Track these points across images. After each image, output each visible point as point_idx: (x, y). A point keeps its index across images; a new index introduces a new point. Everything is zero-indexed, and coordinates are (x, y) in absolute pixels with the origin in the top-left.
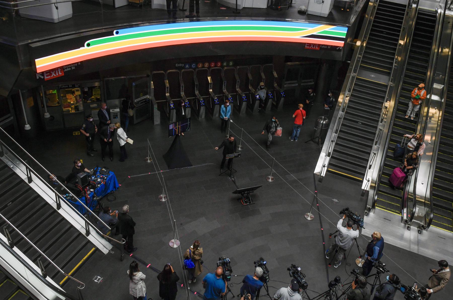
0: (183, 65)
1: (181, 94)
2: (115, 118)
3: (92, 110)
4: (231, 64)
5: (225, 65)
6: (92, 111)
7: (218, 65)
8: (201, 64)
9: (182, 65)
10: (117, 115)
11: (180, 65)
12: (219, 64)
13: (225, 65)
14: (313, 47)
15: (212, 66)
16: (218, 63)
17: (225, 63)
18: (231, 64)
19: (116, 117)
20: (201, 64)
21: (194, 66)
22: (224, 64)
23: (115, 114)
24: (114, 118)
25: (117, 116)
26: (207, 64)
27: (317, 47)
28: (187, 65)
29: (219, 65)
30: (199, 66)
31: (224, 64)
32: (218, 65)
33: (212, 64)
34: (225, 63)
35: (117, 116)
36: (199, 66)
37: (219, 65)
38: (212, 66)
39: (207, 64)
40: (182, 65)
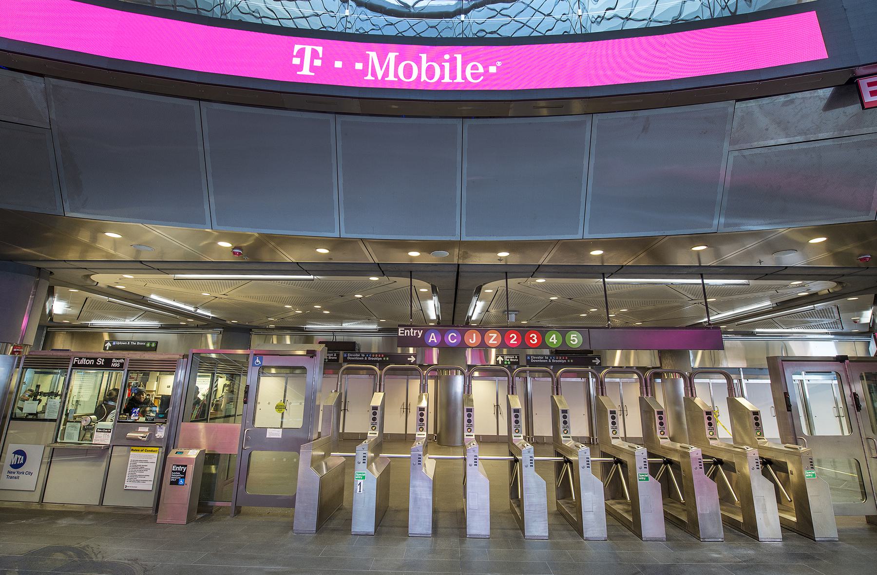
0: (420, 335)
2: (175, 483)
3: (132, 450)
4: (574, 341)
5: (555, 341)
6: (132, 453)
7: (531, 341)
8: (474, 335)
9: (417, 333)
10: (184, 474)
11: (412, 331)
13: (555, 341)
15: (512, 342)
16: (531, 336)
17: (554, 336)
18: (574, 341)
19: (181, 482)
20: (474, 335)
22: (551, 340)
23: (180, 469)
24: (172, 483)
26: (495, 335)
29: (534, 341)
30: (470, 340)
31: (551, 340)
32: (531, 341)
33: (511, 336)
34: (554, 336)
36: (470, 340)
37: (534, 341)
38: (512, 342)
39: (495, 335)
40: (417, 333)
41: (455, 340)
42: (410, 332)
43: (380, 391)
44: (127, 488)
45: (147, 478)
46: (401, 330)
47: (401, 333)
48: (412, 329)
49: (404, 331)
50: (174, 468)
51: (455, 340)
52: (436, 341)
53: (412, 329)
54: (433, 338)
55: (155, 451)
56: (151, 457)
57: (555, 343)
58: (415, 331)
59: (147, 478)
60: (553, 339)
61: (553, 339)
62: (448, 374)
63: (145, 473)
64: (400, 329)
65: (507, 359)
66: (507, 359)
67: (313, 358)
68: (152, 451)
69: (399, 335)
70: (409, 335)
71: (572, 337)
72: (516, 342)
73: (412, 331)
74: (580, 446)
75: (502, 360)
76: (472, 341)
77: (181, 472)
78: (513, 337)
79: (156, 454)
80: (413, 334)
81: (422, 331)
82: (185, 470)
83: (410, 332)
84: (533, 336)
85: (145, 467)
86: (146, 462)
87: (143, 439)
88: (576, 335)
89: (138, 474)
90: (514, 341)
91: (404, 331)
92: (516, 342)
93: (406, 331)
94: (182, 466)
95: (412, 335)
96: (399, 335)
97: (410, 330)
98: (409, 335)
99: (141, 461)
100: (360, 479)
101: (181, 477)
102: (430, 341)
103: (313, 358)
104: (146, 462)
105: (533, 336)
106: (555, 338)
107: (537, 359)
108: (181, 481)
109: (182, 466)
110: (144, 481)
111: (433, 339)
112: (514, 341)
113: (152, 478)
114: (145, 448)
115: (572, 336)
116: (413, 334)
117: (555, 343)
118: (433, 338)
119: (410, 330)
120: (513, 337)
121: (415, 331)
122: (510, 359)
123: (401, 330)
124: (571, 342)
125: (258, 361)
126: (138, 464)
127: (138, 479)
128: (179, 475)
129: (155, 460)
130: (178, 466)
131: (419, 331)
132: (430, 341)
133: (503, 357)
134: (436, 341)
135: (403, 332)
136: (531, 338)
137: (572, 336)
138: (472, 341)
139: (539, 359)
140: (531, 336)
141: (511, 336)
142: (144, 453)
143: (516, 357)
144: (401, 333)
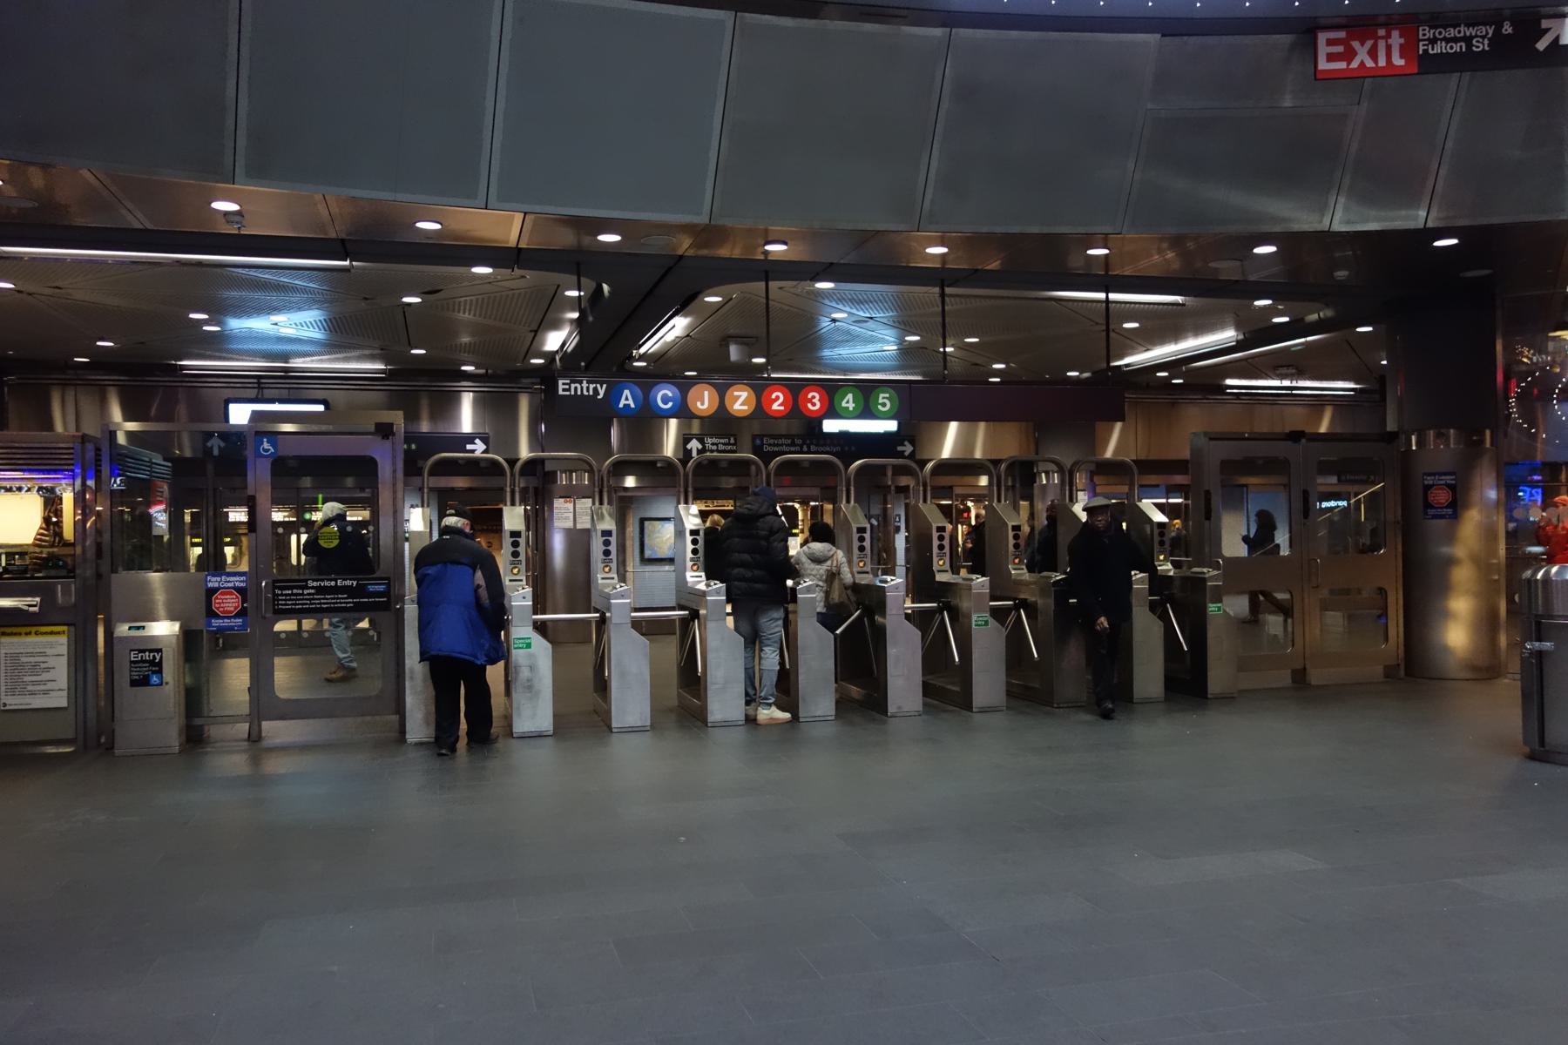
1: (600, 581)
2: (143, 682)
4: (884, 405)
7: (809, 405)
8: (706, 393)
9: (595, 390)
10: (160, 664)
11: (585, 385)
12: (815, 400)
14: (1370, 64)
16: (810, 396)
17: (850, 396)
18: (884, 405)
19: (155, 679)
20: (706, 393)
21: (665, 400)
22: (844, 404)
24: (134, 683)
25: (157, 667)
26: (744, 395)
27: (1401, 57)
28: (627, 392)
29: (814, 404)
30: (699, 404)
31: (844, 404)
32: (809, 405)
33: (774, 396)
34: (850, 396)
35: (160, 672)
36: (699, 404)
37: (814, 404)
38: (775, 407)
39: (744, 395)
40: (595, 390)
41: (670, 404)
42: (582, 388)
43: (513, 504)
44: (8, 708)
45: (50, 686)
46: (564, 384)
47: (564, 390)
48: (585, 382)
49: (569, 384)
50: (132, 656)
51: (670, 404)
52: (633, 406)
53: (585, 382)
54: (627, 399)
55: (59, 633)
56: (52, 645)
57: (851, 409)
58: (592, 386)
59: (50, 686)
60: (848, 402)
61: (848, 402)
62: (571, 480)
63: (45, 676)
64: (560, 382)
65: (713, 444)
66: (713, 444)
67: (388, 438)
68: (52, 633)
69: (561, 392)
70: (579, 393)
71: (880, 398)
72: (782, 408)
73: (585, 385)
74: (889, 580)
75: (700, 447)
76: (703, 404)
77: (152, 662)
78: (778, 398)
79: (63, 639)
80: (588, 390)
81: (605, 386)
82: (158, 658)
83: (582, 388)
84: (814, 397)
85: (43, 665)
86: (44, 654)
87: (31, 609)
88: (887, 395)
89: (26, 679)
90: (779, 405)
91: (569, 384)
92: (782, 408)
93: (573, 386)
94: (151, 651)
95: (585, 393)
96: (561, 392)
97: (581, 383)
98: (579, 393)
99: (32, 655)
100: (522, 648)
101: (154, 672)
102: (621, 406)
103: (388, 438)
104: (44, 654)
105: (814, 397)
106: (851, 400)
107: (778, 445)
108: (155, 679)
109: (151, 651)
110: (46, 692)
111: (627, 402)
112: (779, 405)
113: (65, 686)
114: (34, 629)
115: (882, 395)
116: (588, 390)
117: (851, 409)
118: (627, 399)
119: (581, 383)
120: (778, 398)
121: (592, 386)
122: (717, 444)
123: (564, 384)
124: (880, 407)
125: (266, 445)
126: (24, 659)
127: (30, 688)
128: (145, 668)
129: (64, 650)
130: (143, 651)
131: (598, 386)
132: (621, 406)
133: (701, 441)
134: (633, 406)
135: (567, 387)
136: (810, 401)
137: (882, 395)
138: (703, 404)
139: (782, 445)
140: (810, 396)
141: (774, 396)
142: (32, 639)
143: (732, 441)
144: (564, 390)
